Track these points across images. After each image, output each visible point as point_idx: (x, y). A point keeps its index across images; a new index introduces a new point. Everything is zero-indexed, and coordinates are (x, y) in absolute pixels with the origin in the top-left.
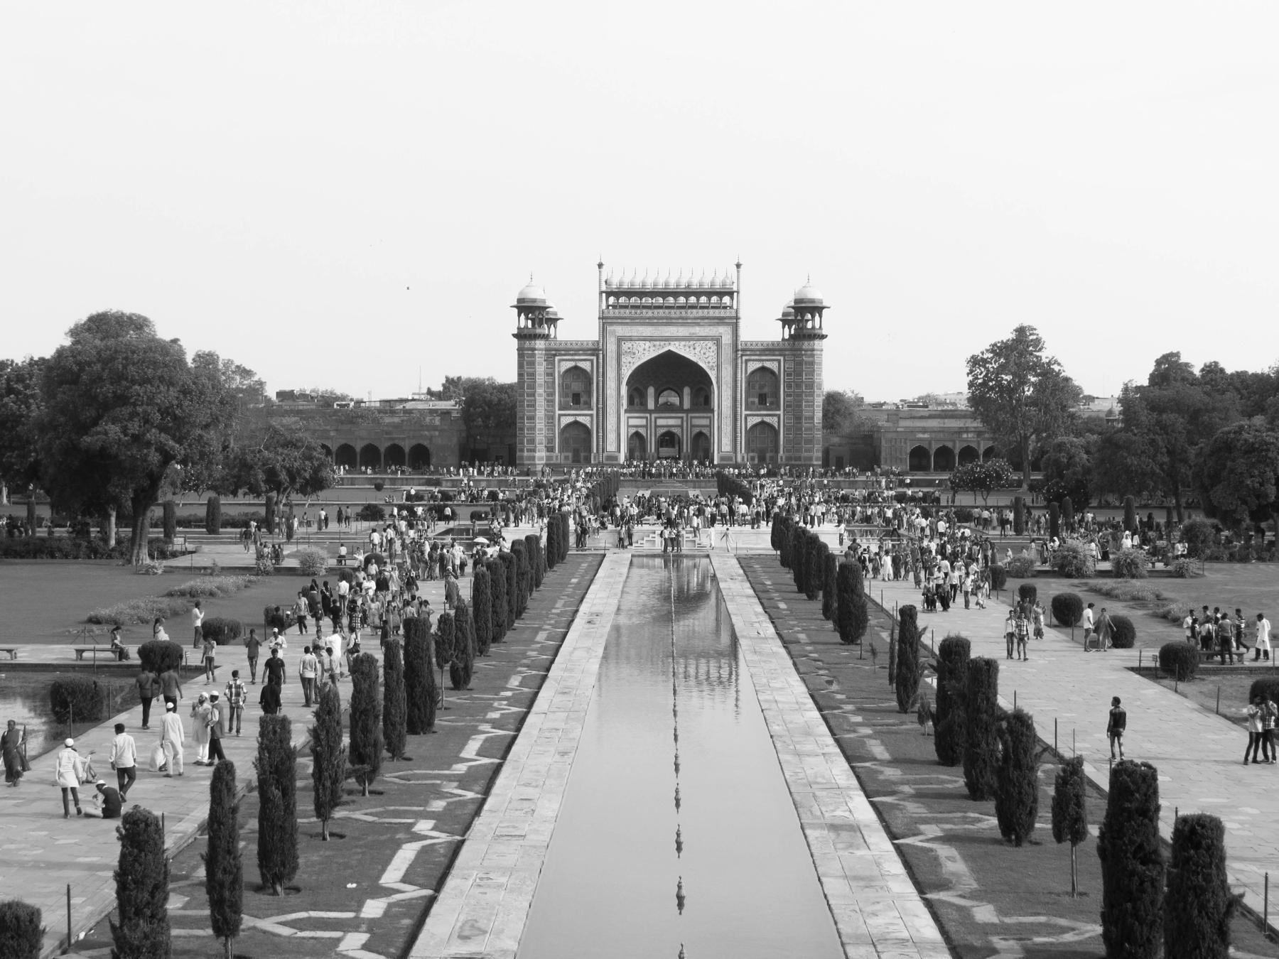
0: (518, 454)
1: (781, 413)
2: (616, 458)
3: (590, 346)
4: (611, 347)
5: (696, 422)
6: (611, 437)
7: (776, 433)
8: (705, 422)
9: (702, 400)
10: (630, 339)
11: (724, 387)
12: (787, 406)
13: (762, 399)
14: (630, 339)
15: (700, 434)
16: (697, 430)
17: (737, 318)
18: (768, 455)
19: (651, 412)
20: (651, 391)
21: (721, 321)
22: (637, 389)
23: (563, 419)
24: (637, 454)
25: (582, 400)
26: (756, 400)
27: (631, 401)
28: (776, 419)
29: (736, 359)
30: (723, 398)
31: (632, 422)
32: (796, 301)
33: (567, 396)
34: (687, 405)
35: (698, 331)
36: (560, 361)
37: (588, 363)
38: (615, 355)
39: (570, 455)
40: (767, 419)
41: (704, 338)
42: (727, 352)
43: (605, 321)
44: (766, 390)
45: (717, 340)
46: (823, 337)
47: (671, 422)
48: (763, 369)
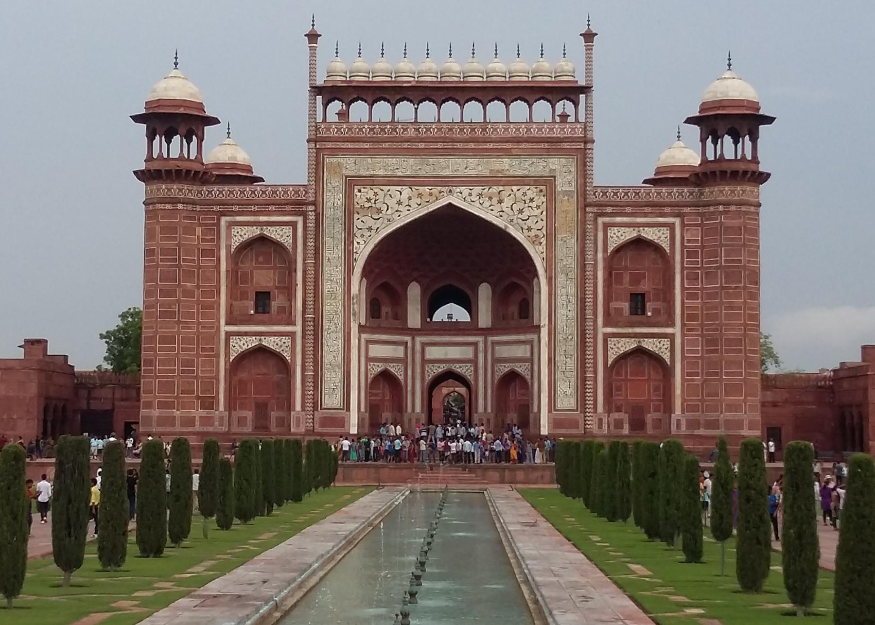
0: (143, 412)
1: (677, 330)
2: (342, 422)
3: (291, 196)
4: (333, 199)
5: (504, 352)
6: (332, 378)
7: (666, 371)
8: (521, 351)
9: (514, 309)
10: (371, 181)
11: (561, 279)
12: (689, 317)
13: (638, 302)
14: (371, 181)
15: (512, 377)
16: (505, 368)
17: (587, 141)
18: (649, 418)
19: (413, 332)
20: (414, 291)
21: (552, 145)
22: (385, 287)
23: (233, 341)
24: (386, 415)
25: (275, 305)
26: (626, 306)
27: (374, 310)
28: (666, 343)
29: (584, 222)
30: (557, 300)
31: (376, 351)
32: (704, 107)
33: (244, 296)
34: (485, 319)
35: (506, 165)
36: (231, 225)
37: (288, 230)
38: (340, 214)
39: (249, 414)
40: (649, 345)
41: (521, 181)
42: (568, 207)
43: (321, 144)
44: (644, 287)
45: (547, 183)
46: (762, 178)
47: (454, 353)
48: (639, 243)
